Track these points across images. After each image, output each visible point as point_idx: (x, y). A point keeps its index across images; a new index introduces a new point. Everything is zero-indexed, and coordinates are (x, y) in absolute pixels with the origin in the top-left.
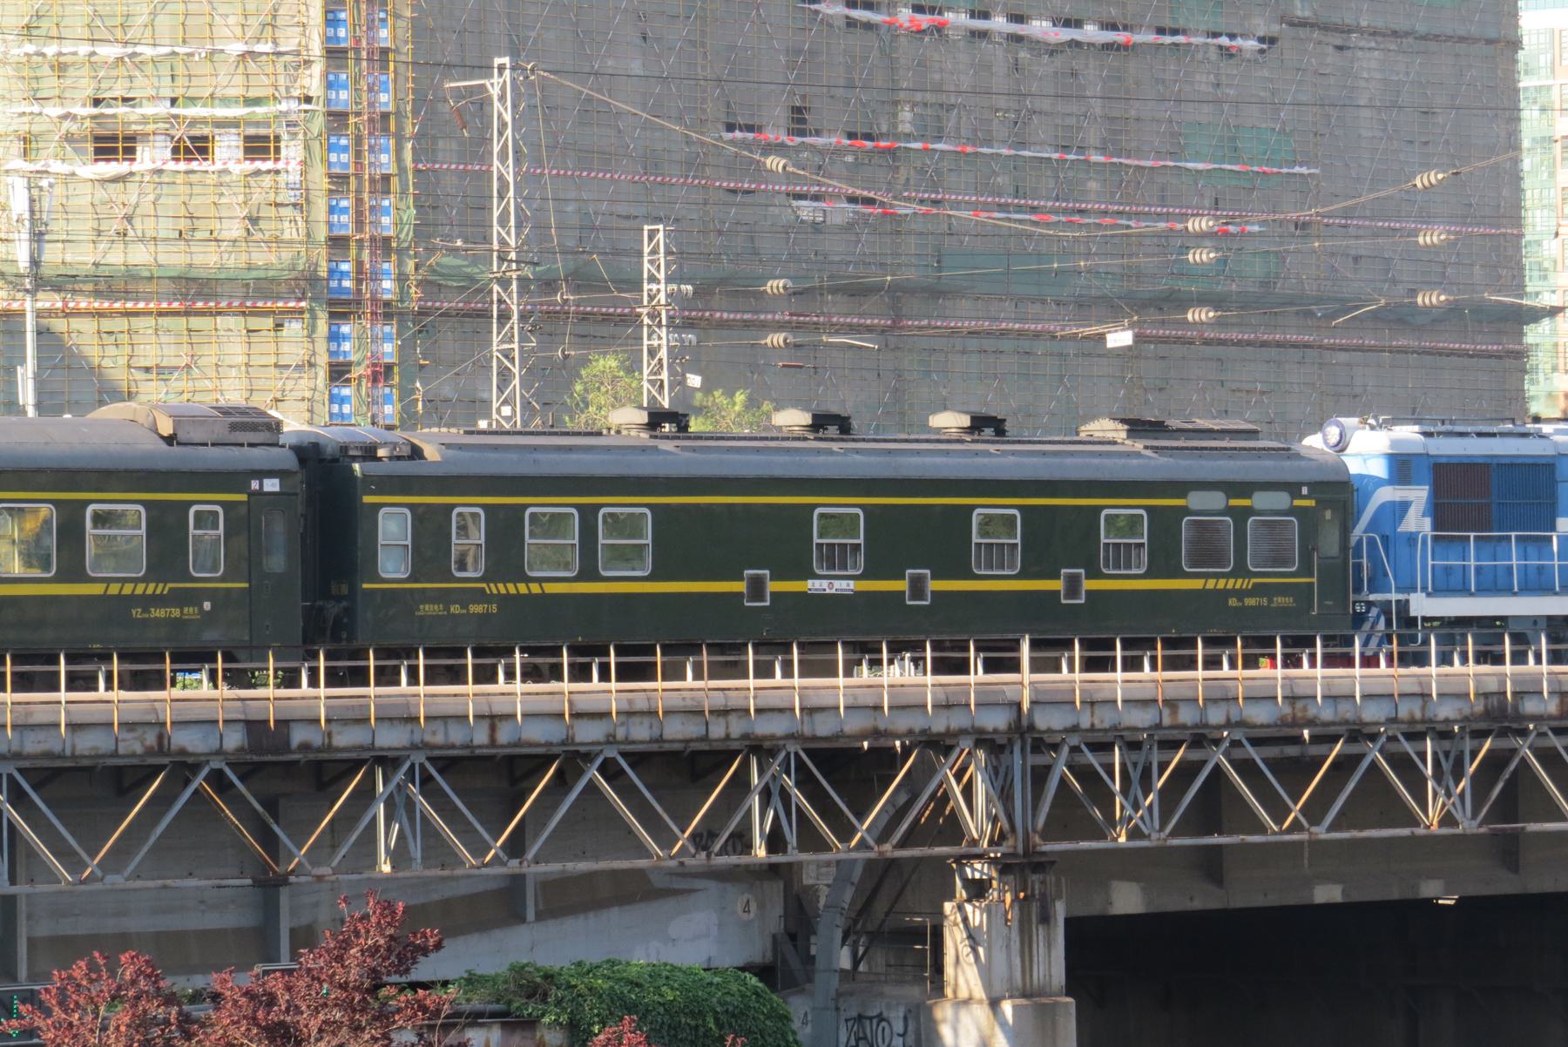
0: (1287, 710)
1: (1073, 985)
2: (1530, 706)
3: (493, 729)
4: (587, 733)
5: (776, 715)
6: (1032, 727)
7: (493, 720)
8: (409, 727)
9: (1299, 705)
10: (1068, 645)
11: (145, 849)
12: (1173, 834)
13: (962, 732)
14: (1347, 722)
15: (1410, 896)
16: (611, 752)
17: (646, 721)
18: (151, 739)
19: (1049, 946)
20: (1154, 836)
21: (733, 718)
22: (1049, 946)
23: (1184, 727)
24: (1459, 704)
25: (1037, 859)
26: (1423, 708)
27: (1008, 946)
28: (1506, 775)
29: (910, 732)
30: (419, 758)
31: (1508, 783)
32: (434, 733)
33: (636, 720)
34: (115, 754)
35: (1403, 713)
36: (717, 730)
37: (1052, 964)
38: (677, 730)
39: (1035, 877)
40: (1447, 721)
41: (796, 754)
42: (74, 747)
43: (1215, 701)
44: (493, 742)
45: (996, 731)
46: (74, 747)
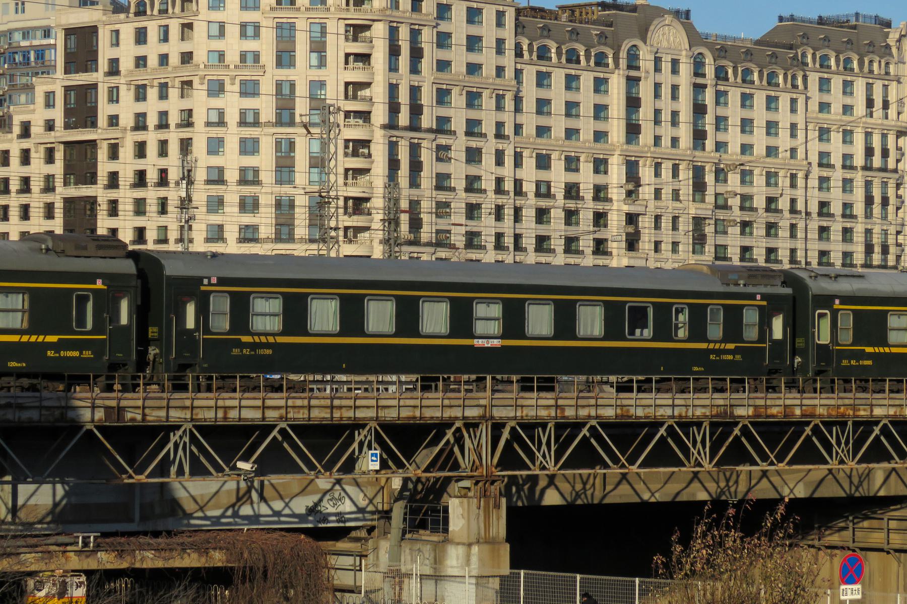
0: (619, 411)
1: (510, 537)
2: (740, 412)
3: (225, 413)
4: (272, 415)
5: (365, 409)
6: (492, 418)
7: (225, 407)
8: (184, 411)
9: (625, 408)
10: (438, 379)
11: (53, 466)
12: (559, 469)
13: (457, 418)
14: (646, 417)
15: (691, 499)
16: (283, 425)
17: (301, 411)
18: (57, 413)
19: (498, 519)
20: (552, 469)
21: (344, 410)
22: (498, 519)
23: (567, 418)
24: (703, 410)
25: (493, 478)
26: (687, 412)
27: (478, 518)
28: (727, 443)
29: (432, 418)
30: (188, 426)
31: (727, 447)
32: (197, 414)
33: (296, 410)
34: (39, 421)
35: (676, 413)
36: (337, 415)
37: (500, 527)
38: (316, 414)
39: (492, 487)
40: (698, 417)
41: (375, 428)
42: (20, 418)
43: (583, 406)
44: (225, 418)
45: (474, 418)
46: (20, 418)
